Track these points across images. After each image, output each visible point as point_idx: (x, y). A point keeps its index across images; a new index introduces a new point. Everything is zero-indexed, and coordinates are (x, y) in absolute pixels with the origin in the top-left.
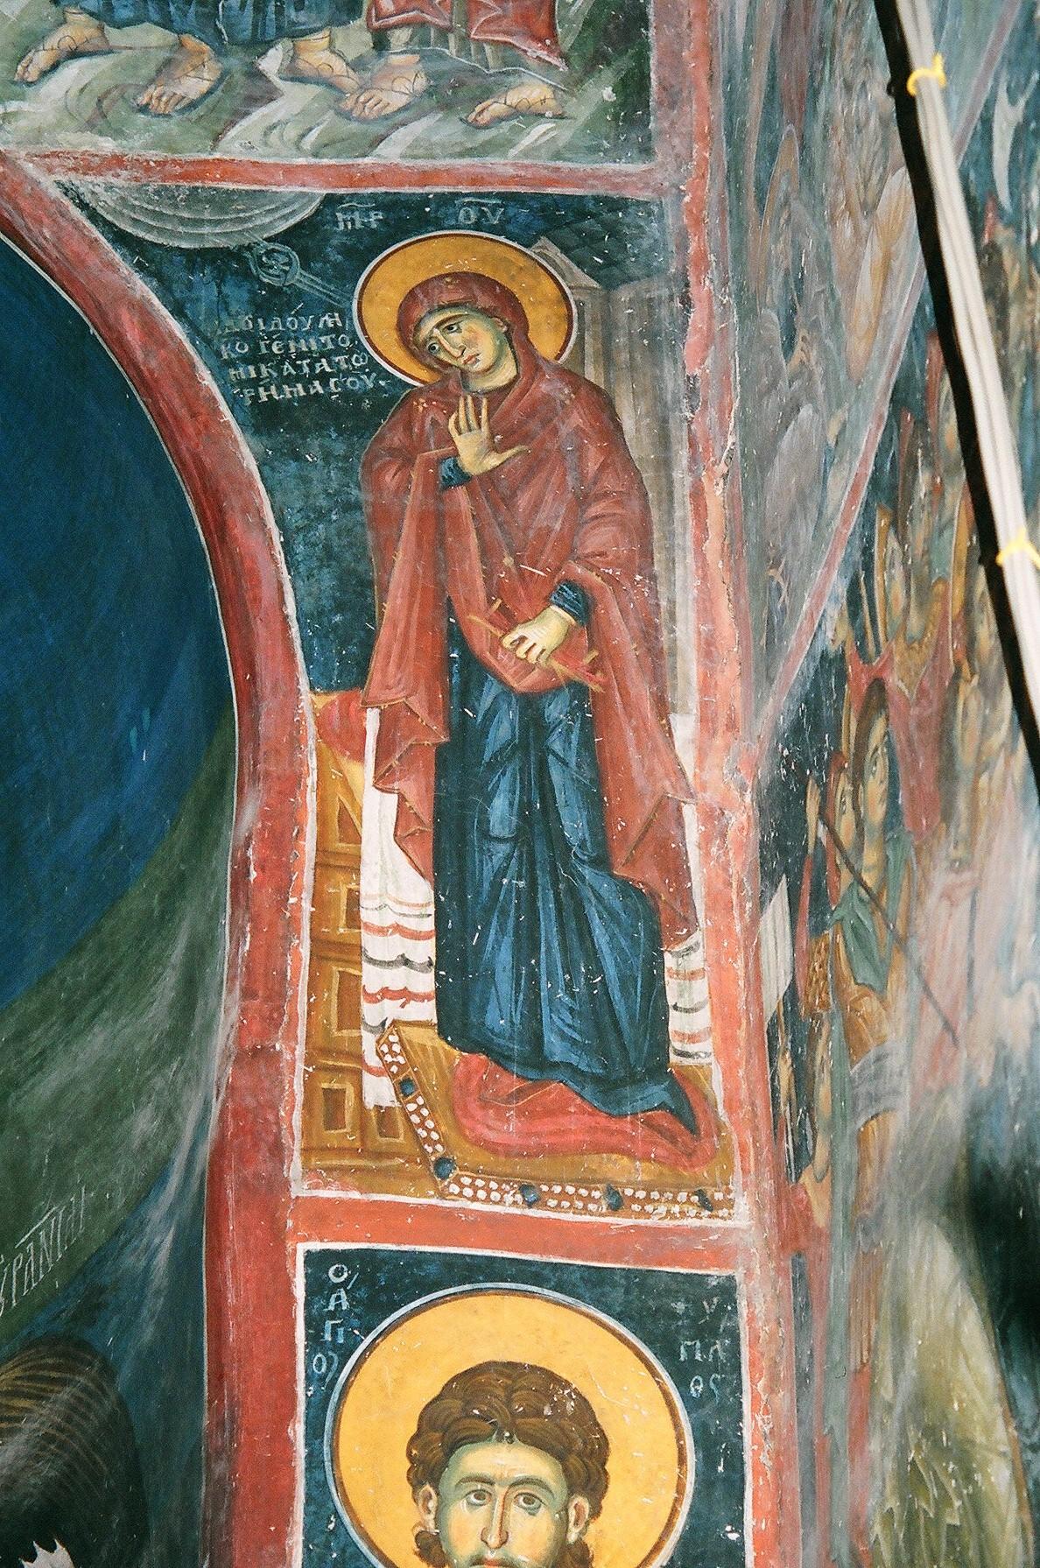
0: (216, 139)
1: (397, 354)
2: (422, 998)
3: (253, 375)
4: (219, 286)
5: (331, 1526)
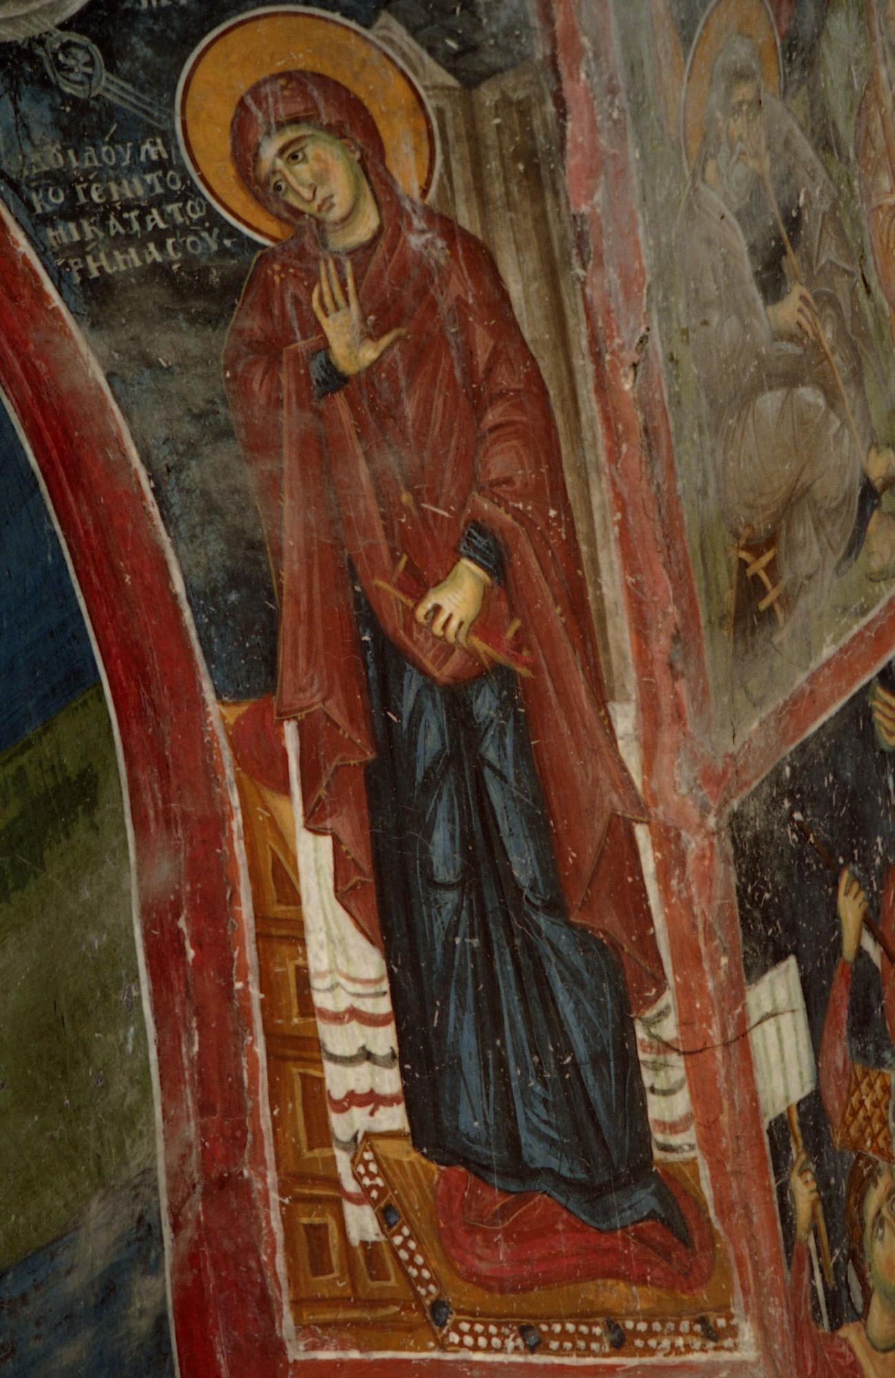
1: (238, 199)
2: (388, 1101)
3: (76, 237)
4: (15, 103)
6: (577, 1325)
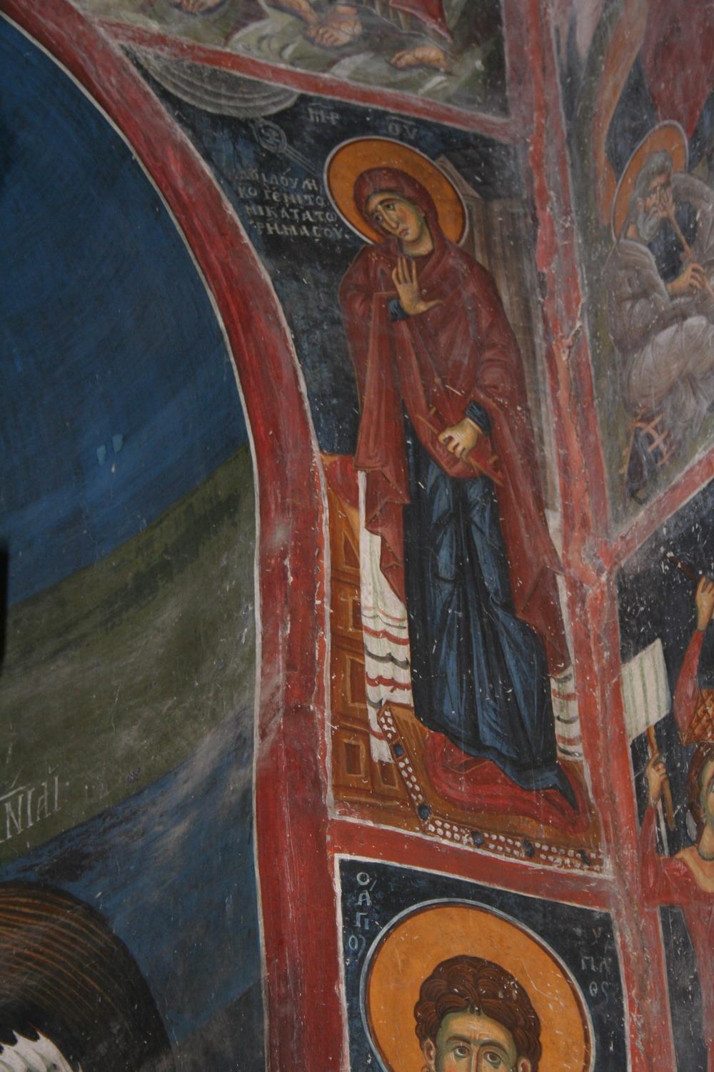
0: (227, 37)
1: (355, 217)
2: (403, 687)
3: (262, 213)
4: (234, 144)
5: (369, 1061)
6: (506, 838)
